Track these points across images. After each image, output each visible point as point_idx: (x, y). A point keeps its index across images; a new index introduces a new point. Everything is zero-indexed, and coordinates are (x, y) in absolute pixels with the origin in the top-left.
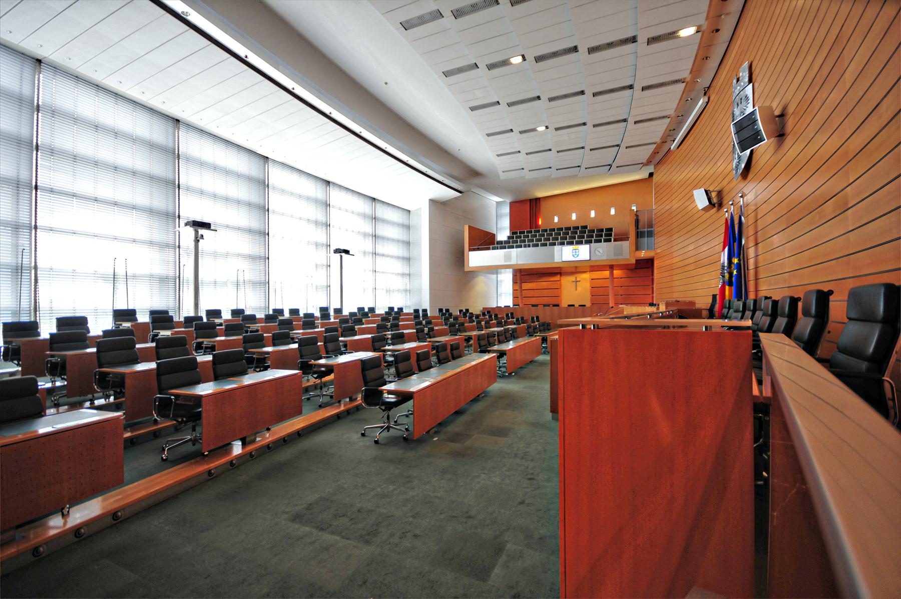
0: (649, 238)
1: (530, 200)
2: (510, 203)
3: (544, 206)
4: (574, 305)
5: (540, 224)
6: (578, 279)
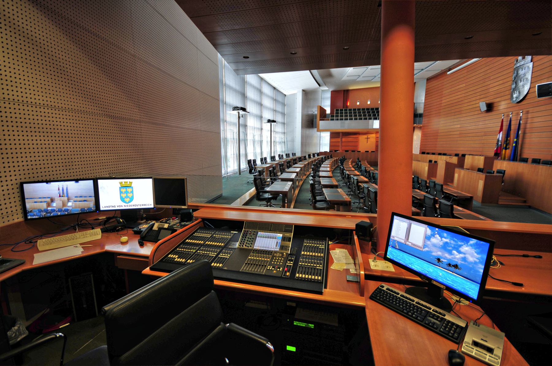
0: (420, 118)
1: (344, 91)
2: (331, 91)
3: (351, 95)
4: (368, 151)
5: (348, 105)
6: (369, 137)
